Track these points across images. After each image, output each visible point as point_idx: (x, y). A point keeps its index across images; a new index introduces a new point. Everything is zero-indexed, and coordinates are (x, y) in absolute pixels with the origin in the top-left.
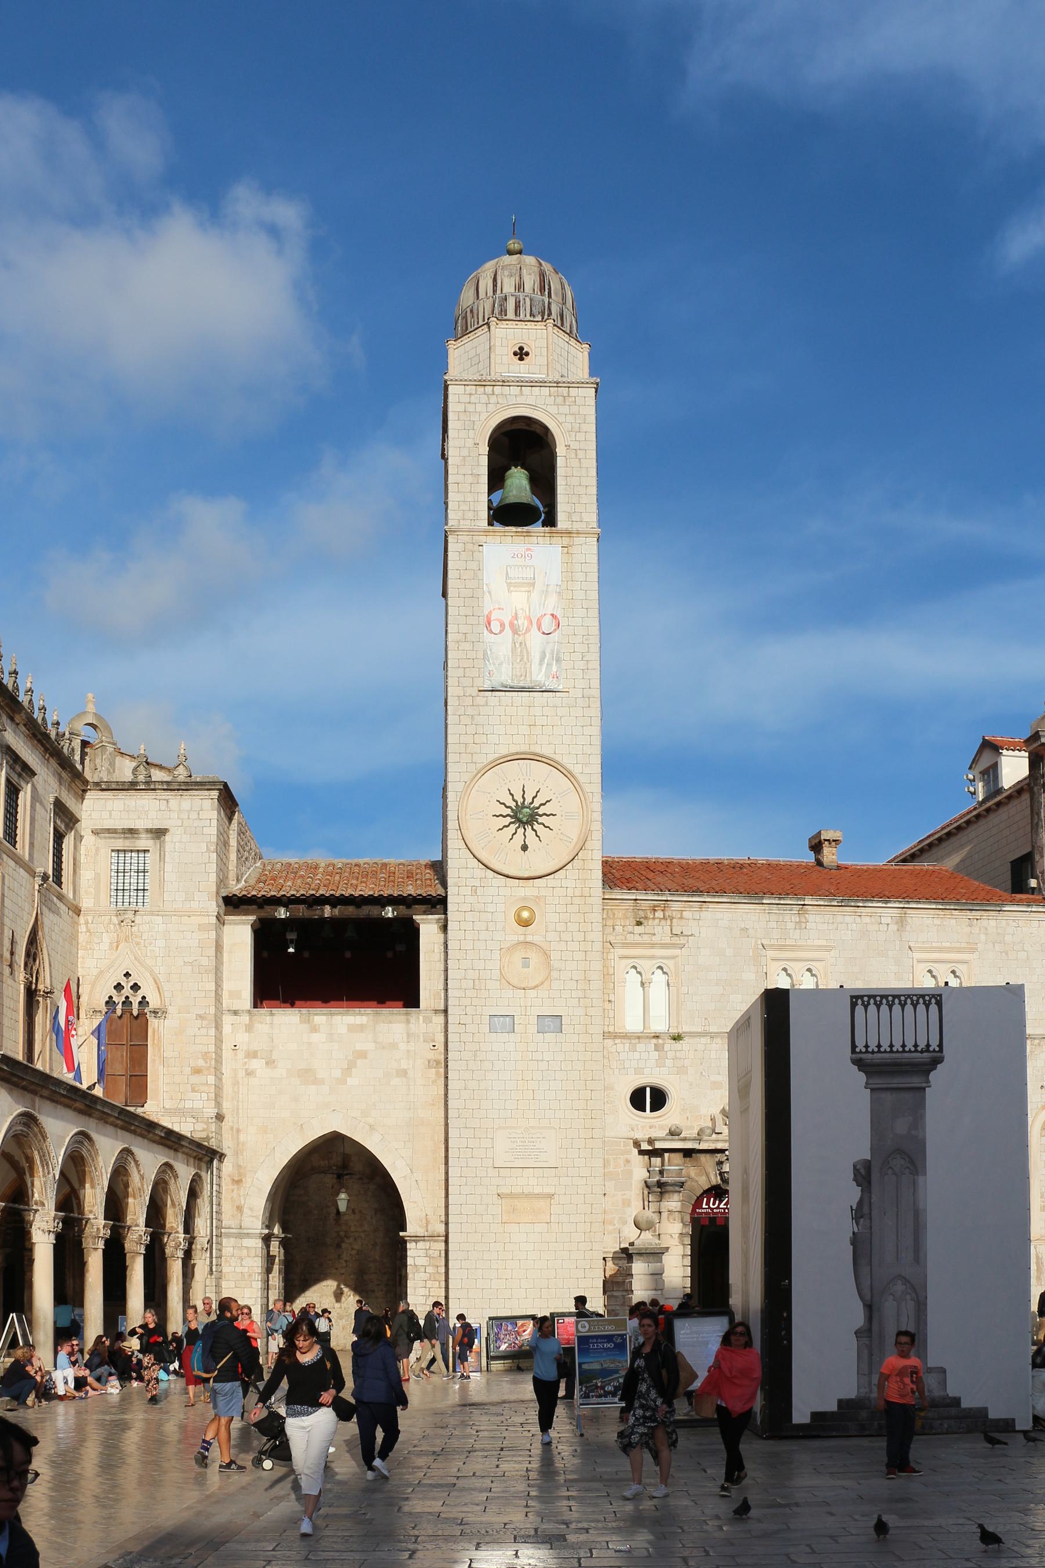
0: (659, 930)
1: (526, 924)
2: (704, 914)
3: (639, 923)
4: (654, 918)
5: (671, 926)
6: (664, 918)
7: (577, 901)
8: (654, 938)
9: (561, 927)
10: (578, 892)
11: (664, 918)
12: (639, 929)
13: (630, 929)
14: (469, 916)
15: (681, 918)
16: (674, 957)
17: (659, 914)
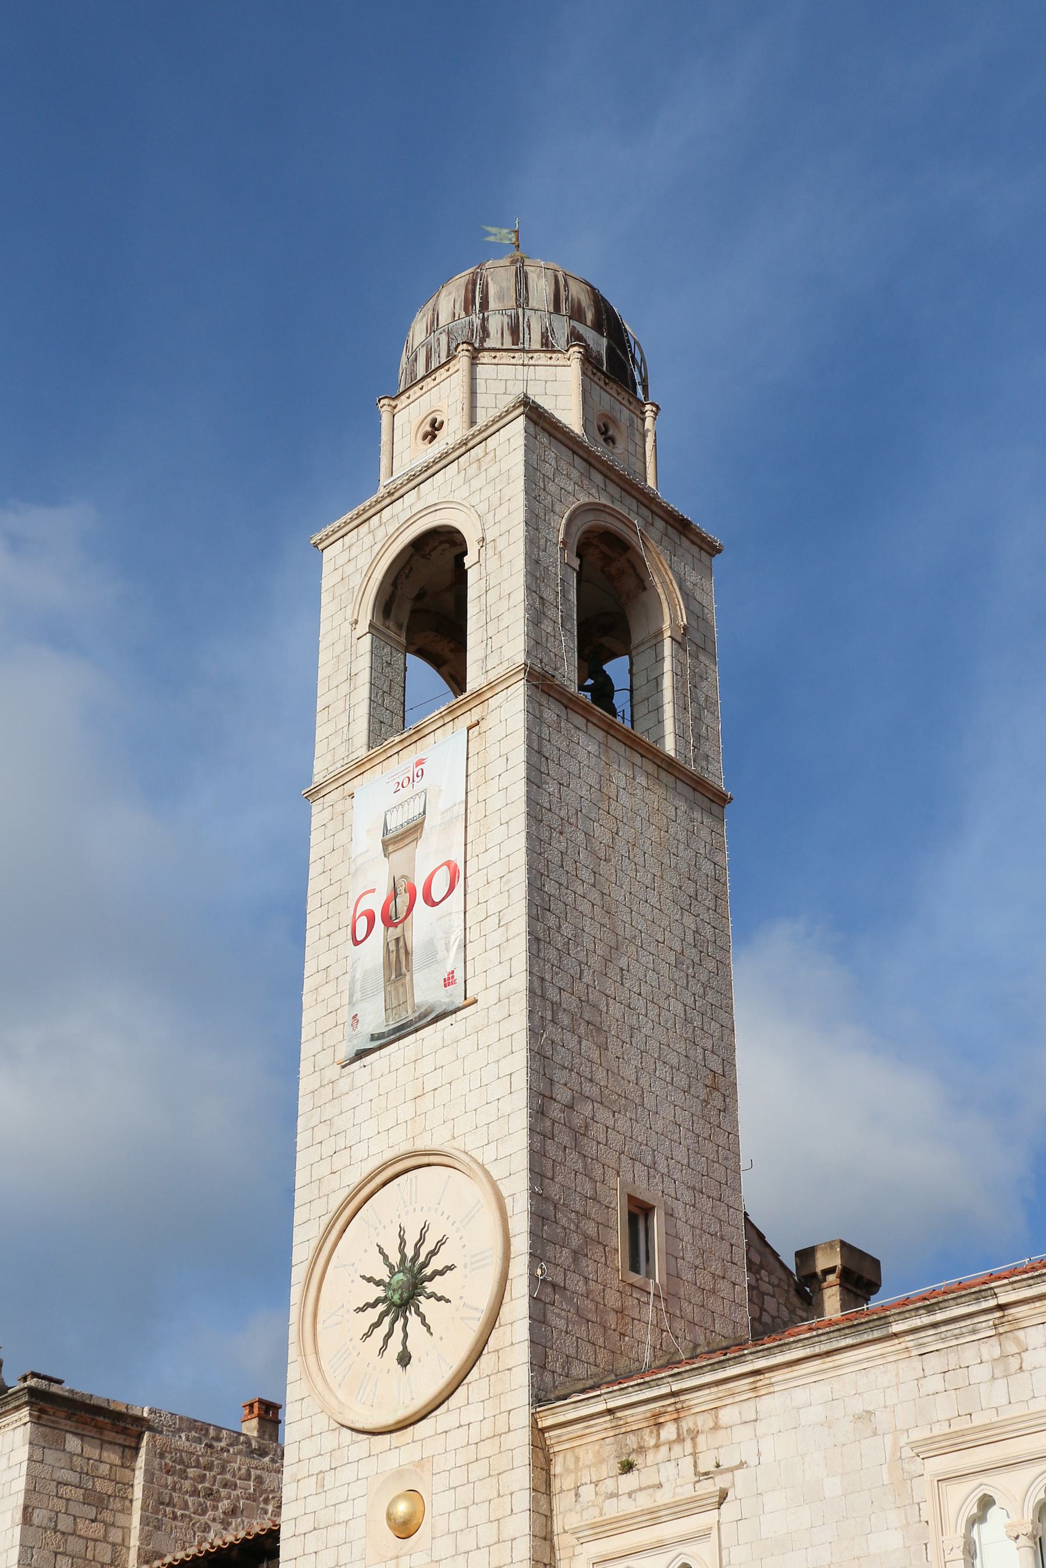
0: (668, 1473)
1: (405, 1529)
2: (766, 1404)
3: (628, 1467)
4: (657, 1446)
5: (694, 1454)
6: (680, 1439)
7: (486, 1449)
8: (659, 1493)
9: (457, 1521)
10: (487, 1430)
11: (680, 1439)
12: (629, 1481)
13: (609, 1485)
14: (312, 1542)
15: (716, 1427)
16: (702, 1535)
17: (669, 1432)
